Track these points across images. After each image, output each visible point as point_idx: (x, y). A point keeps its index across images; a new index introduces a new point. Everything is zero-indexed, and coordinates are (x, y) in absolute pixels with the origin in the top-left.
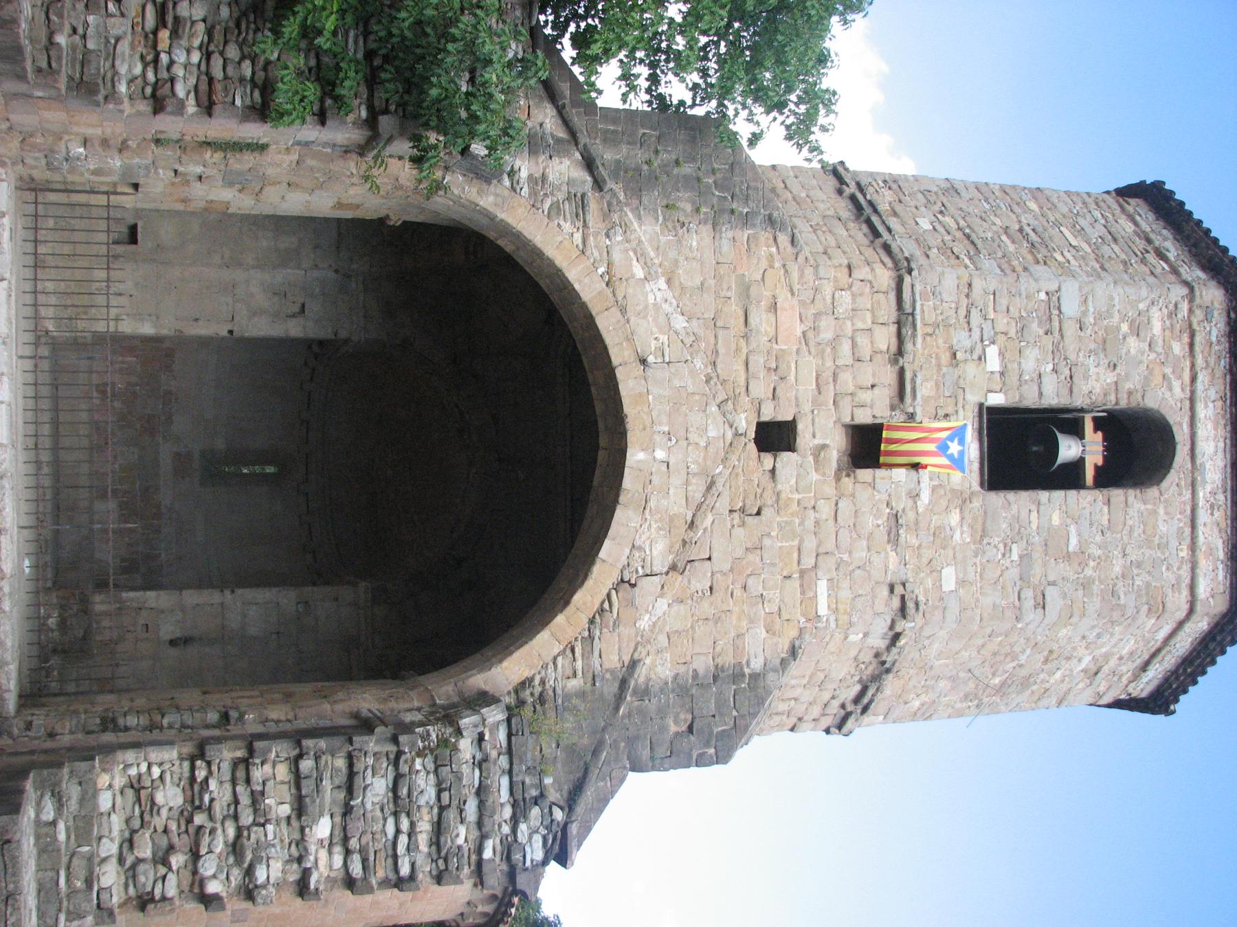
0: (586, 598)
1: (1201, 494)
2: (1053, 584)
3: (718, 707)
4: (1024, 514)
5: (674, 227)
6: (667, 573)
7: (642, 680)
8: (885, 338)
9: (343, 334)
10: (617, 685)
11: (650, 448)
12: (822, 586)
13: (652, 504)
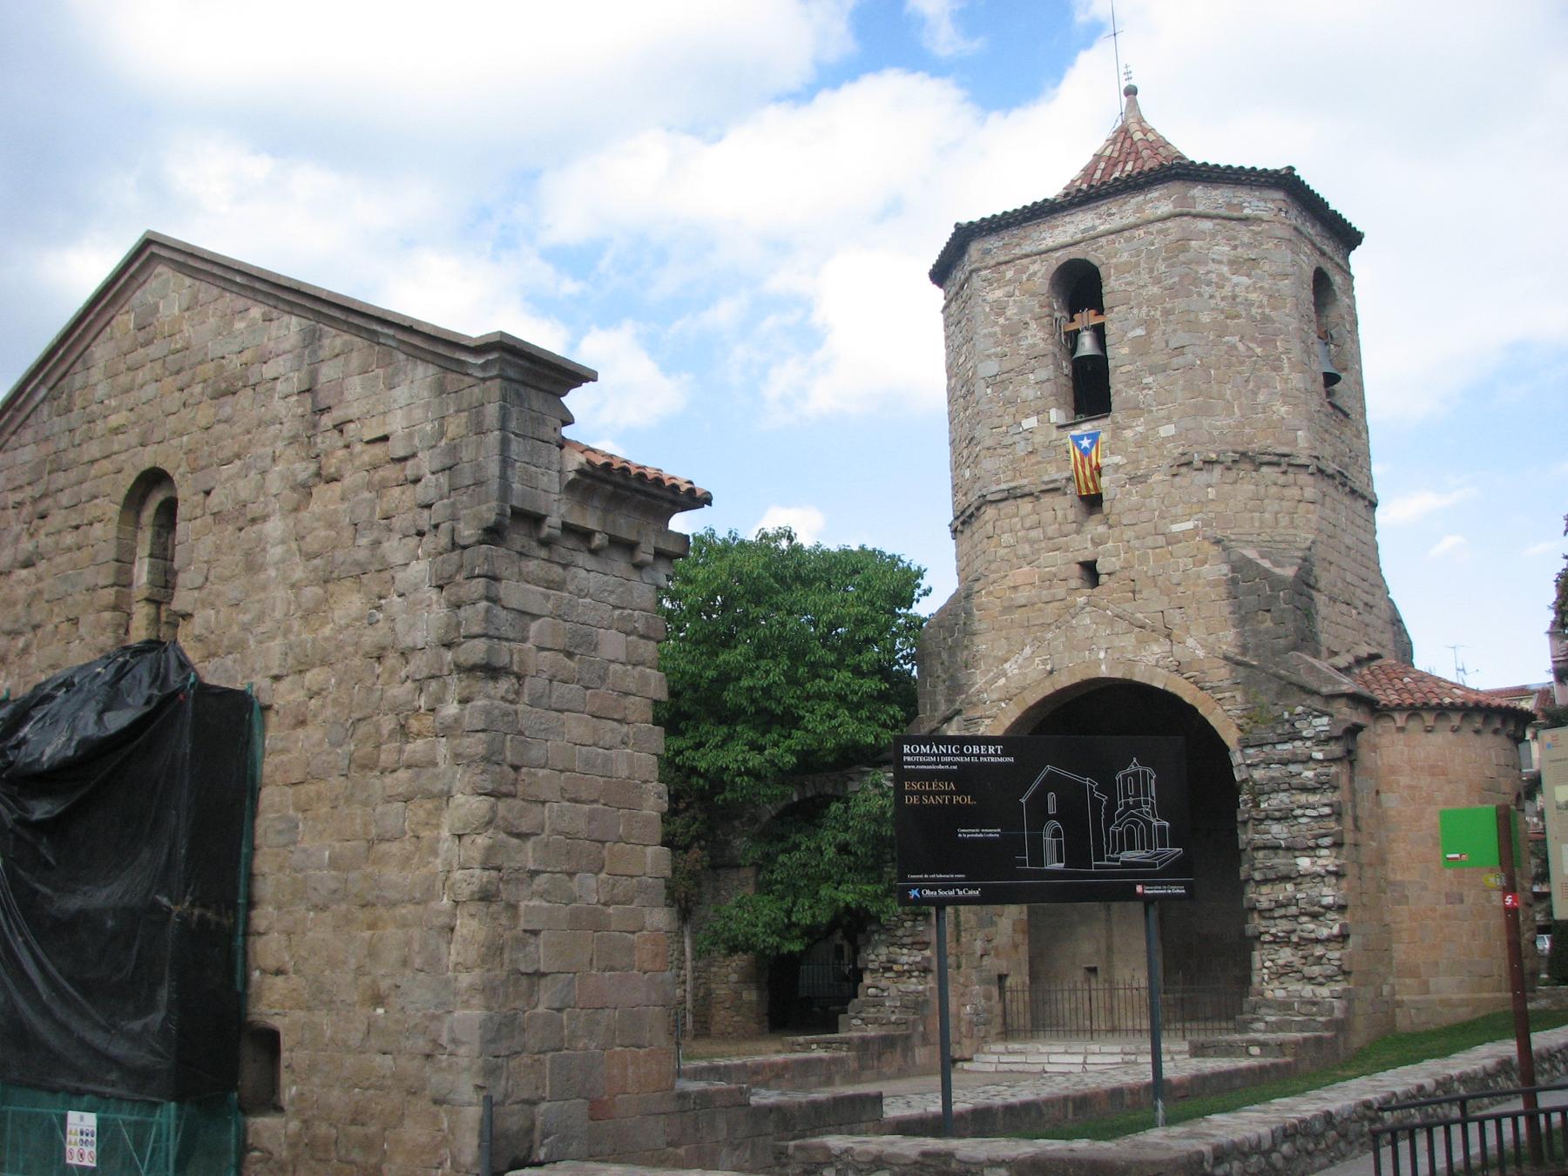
0: (1188, 693)
1: (1102, 227)
2: (1167, 343)
3: (1251, 594)
4: (1123, 378)
7: (1236, 650)
8: (1026, 506)
11: (1098, 662)
12: (1176, 528)
13: (1130, 656)
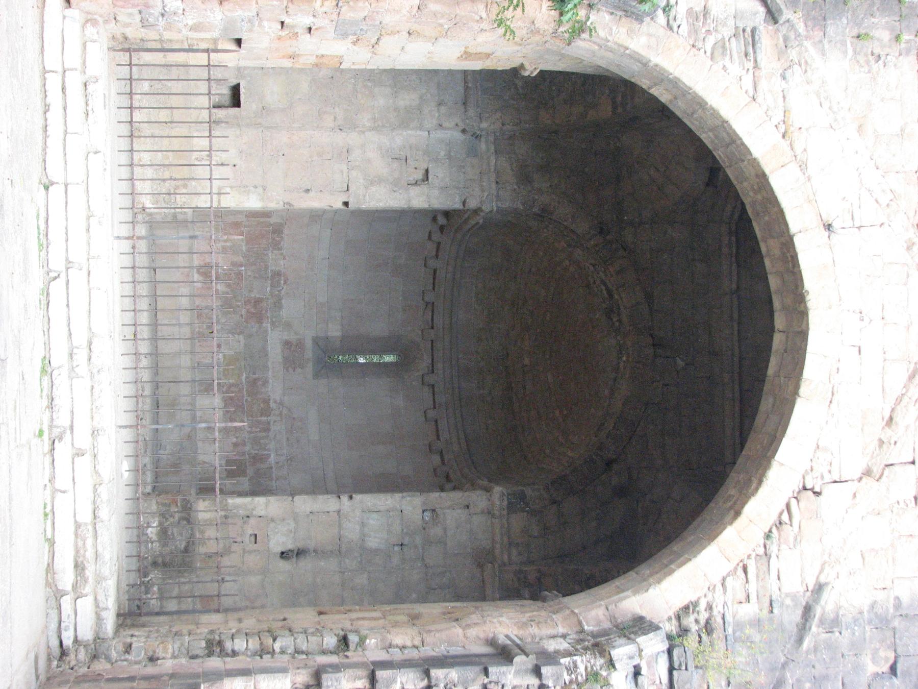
5: (868, 62)
6: (860, 479)
9: (473, 204)
10: (799, 612)
